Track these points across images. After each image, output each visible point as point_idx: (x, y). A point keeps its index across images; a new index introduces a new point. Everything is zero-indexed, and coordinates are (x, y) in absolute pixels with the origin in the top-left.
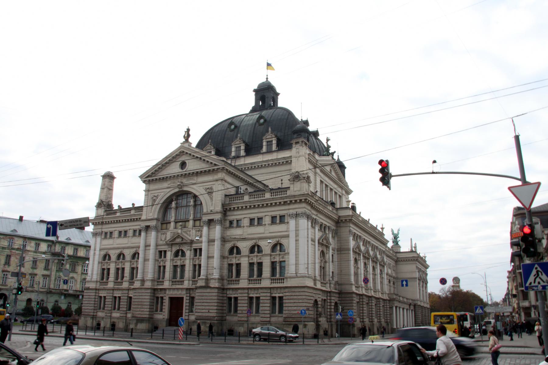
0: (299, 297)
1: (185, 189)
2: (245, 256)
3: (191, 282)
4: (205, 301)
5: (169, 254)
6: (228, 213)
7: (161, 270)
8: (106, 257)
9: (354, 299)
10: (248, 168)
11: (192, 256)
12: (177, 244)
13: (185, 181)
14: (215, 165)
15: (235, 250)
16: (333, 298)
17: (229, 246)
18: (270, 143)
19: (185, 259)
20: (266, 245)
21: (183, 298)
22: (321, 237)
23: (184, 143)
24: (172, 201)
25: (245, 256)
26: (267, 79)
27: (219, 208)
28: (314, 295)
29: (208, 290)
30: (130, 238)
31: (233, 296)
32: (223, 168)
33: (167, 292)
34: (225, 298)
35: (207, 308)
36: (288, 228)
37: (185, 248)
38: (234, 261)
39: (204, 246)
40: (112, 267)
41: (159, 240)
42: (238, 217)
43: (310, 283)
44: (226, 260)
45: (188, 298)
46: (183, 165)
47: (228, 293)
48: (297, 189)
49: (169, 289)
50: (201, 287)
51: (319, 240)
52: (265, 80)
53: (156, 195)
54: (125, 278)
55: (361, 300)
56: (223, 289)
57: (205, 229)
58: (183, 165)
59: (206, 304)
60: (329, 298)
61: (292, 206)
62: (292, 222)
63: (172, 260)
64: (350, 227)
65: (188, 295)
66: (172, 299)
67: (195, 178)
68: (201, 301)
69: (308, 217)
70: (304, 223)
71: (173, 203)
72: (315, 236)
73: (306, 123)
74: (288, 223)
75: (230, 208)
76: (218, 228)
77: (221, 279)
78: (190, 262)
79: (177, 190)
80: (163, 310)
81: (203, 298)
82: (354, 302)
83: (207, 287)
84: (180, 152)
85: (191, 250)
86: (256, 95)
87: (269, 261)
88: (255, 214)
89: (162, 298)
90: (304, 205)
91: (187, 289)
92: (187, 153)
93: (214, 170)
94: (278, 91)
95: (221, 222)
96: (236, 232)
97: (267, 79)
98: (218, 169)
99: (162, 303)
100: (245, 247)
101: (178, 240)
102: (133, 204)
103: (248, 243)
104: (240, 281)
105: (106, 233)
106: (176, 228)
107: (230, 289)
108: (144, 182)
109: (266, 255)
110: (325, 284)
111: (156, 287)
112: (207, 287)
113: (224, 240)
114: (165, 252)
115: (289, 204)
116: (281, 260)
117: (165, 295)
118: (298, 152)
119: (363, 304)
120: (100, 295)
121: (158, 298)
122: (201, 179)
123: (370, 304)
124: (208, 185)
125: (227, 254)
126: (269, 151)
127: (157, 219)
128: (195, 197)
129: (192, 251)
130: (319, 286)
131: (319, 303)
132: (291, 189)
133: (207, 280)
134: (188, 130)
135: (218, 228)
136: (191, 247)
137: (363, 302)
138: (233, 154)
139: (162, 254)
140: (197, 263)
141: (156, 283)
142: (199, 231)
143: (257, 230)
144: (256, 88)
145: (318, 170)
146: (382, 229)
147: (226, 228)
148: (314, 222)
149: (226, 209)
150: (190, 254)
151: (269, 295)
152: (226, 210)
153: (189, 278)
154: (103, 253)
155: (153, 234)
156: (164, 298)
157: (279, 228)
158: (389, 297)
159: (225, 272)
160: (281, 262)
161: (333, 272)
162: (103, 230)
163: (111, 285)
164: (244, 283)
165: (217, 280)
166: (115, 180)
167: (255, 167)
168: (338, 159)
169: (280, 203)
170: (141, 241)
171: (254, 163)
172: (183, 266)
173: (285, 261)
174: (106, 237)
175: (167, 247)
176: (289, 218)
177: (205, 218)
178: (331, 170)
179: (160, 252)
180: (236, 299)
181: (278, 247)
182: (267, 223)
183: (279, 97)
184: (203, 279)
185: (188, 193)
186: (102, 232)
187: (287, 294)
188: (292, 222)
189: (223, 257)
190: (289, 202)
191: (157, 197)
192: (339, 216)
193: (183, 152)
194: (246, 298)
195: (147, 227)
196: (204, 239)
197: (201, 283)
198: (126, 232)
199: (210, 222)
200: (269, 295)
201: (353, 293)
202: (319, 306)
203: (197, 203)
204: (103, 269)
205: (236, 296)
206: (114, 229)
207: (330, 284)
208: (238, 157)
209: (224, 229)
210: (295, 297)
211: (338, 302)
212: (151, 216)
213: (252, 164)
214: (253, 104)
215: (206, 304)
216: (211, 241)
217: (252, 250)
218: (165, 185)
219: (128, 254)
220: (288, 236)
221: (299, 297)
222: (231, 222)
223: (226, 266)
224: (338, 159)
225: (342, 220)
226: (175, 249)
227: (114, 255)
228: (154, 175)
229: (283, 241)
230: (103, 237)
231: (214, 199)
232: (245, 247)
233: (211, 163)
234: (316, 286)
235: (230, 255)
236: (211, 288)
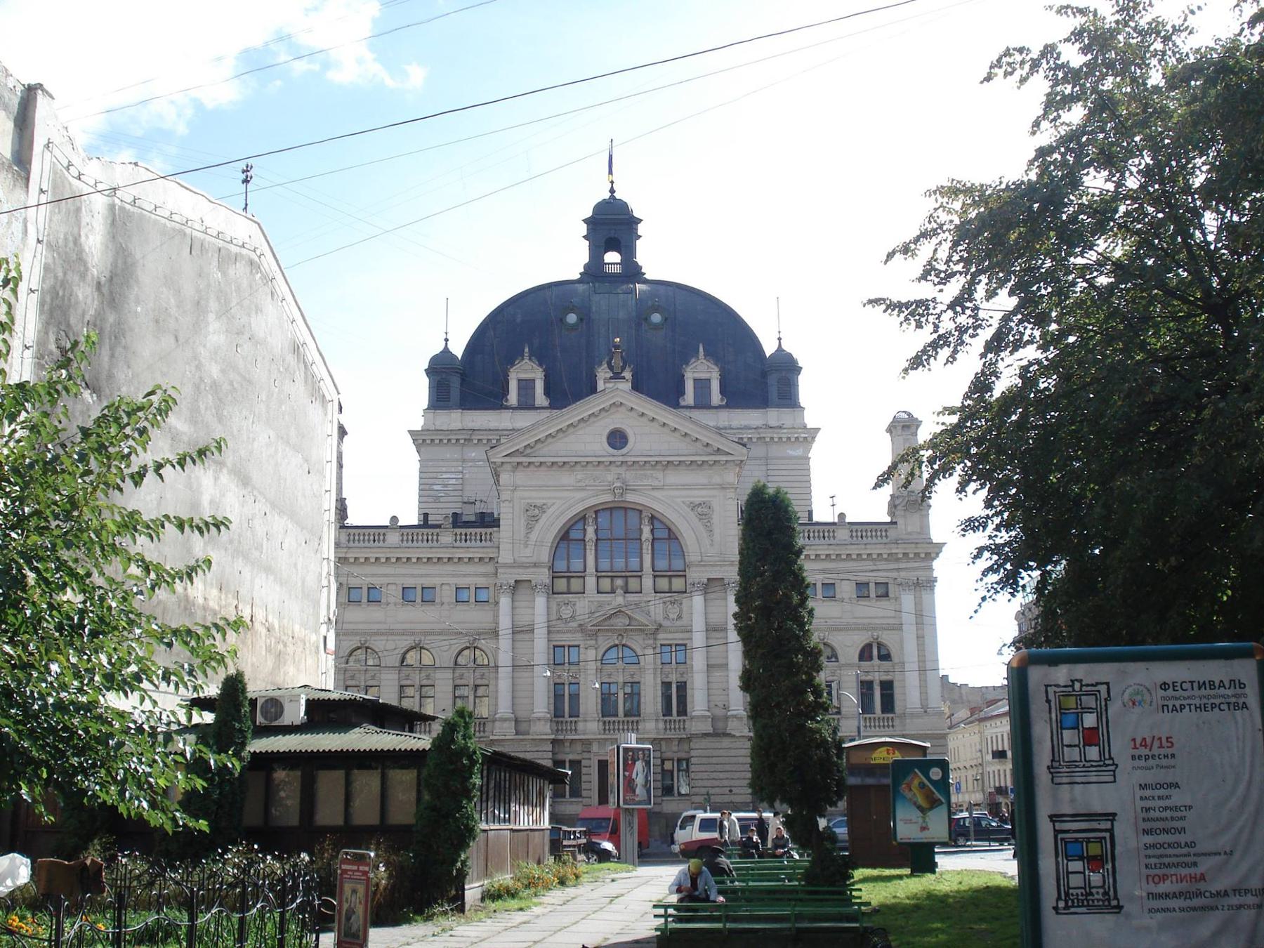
1: (631, 497)
3: (661, 725)
4: (719, 767)
13: (629, 476)
26: (612, 191)
29: (726, 742)
30: (391, 607)
33: (595, 748)
35: (726, 783)
37: (636, 643)
46: (617, 439)
52: (607, 195)
53: (539, 502)
58: (617, 439)
59: (721, 775)
62: (907, 600)
67: (660, 475)
68: (708, 768)
79: (606, 498)
80: (584, 793)
81: (714, 760)
87: (854, 679)
97: (612, 191)
101: (620, 622)
112: (719, 734)
115: (898, 560)
117: (586, 755)
122: (673, 477)
124: (698, 496)
140: (673, 678)
142: (673, 603)
144: (589, 214)
155: (540, 601)
156: (584, 763)
175: (579, 636)
183: (638, 242)
191: (542, 509)
203: (667, 536)
206: (386, 580)
212: (526, 554)
215: (721, 775)
217: (865, 654)
218: (567, 478)
220: (899, 627)
226: (604, 643)
229: (887, 638)
231: (717, 531)
236: (729, 735)
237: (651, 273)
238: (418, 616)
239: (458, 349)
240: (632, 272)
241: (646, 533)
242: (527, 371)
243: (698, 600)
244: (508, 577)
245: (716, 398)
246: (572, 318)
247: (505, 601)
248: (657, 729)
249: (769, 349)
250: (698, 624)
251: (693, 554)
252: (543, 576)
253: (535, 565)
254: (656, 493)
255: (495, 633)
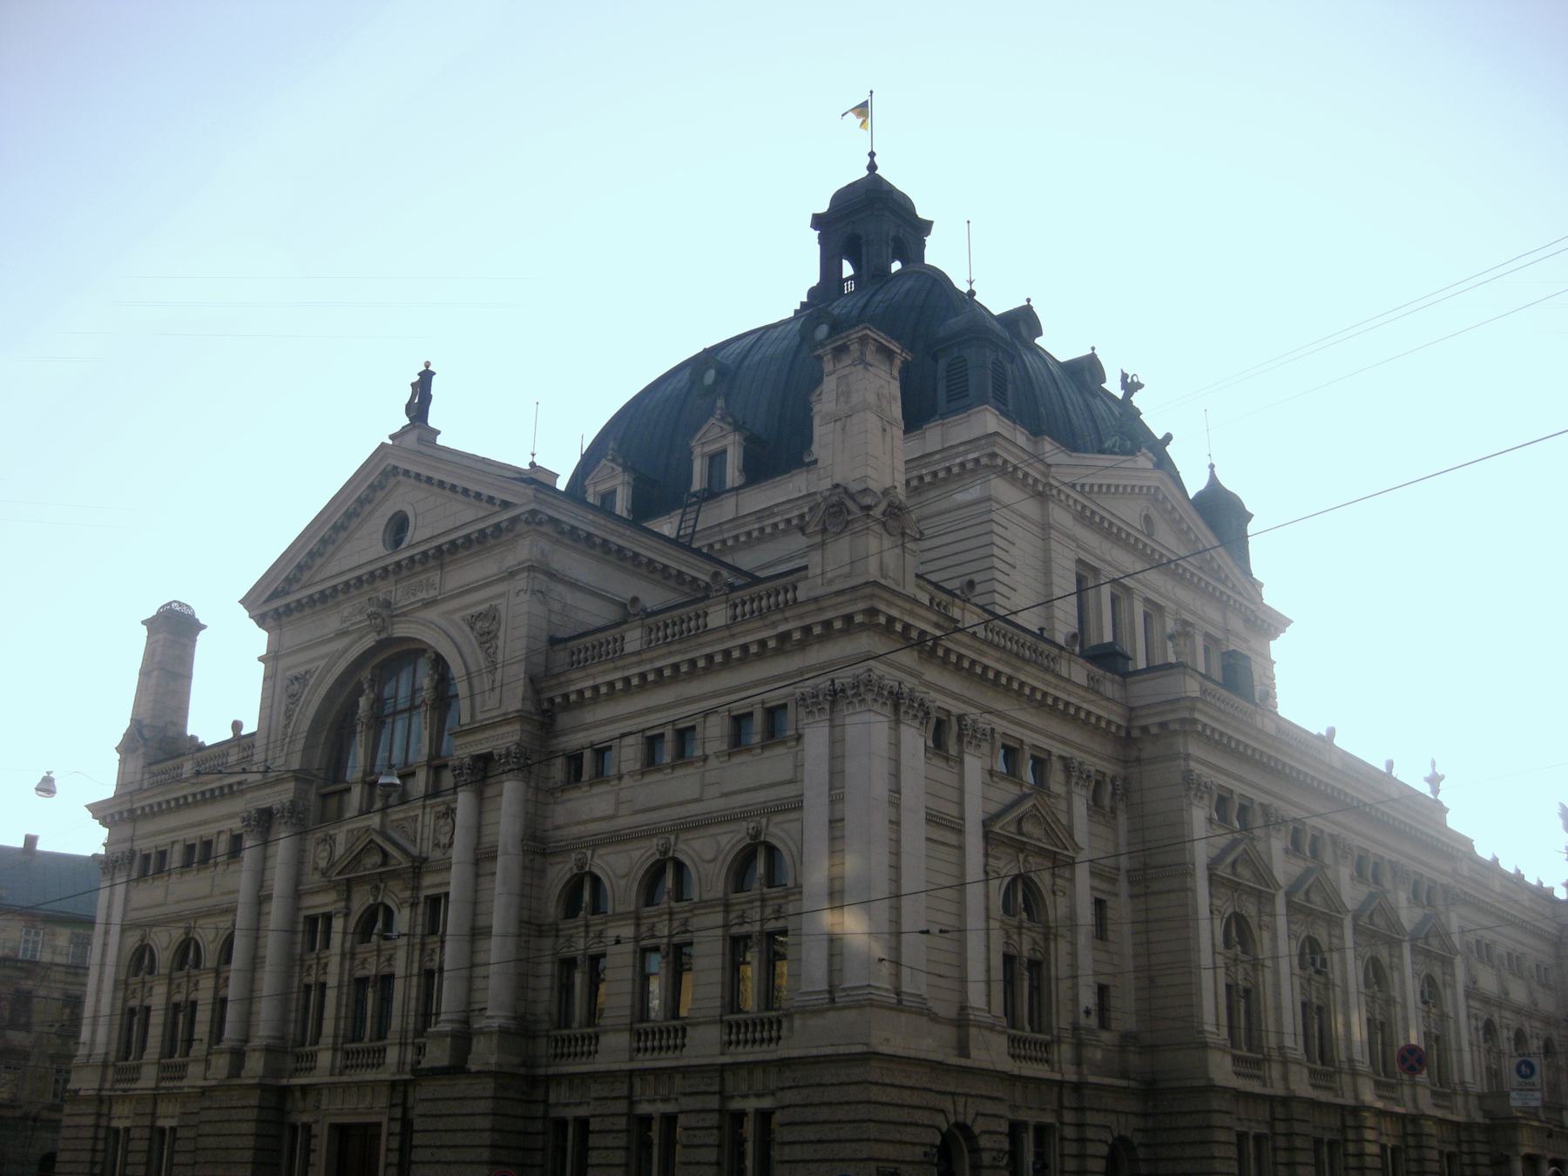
0: (841, 1114)
1: (400, 630)
2: (623, 916)
5: (338, 924)
6: (564, 720)
7: (305, 999)
8: (141, 960)
9: (1217, 1120)
10: (749, 534)
11: (419, 930)
12: (361, 880)
13: (398, 593)
14: (506, 505)
15: (582, 893)
16: (1097, 1118)
17: (560, 872)
19: (395, 948)
20: (708, 857)
21: (379, 1125)
22: (1225, 851)
23: (404, 431)
24: (359, 691)
25: (623, 916)
26: (872, 167)
27: (515, 698)
28: (948, 1104)
31: (570, 1113)
32: (534, 512)
34: (539, 1126)
36: (798, 766)
38: (581, 946)
39: (456, 882)
40: (158, 998)
41: (308, 868)
42: (599, 735)
43: (931, 1044)
44: (548, 943)
45: (397, 1127)
46: (398, 527)
47: (552, 1099)
48: (836, 563)
49: (332, 1086)
50: (435, 1072)
51: (987, 824)
54: (196, 1046)
55: (1281, 1127)
56: (533, 1081)
57: (464, 802)
58: (398, 527)
60: (1069, 1117)
61: (817, 655)
63: (348, 955)
64: (1188, 757)
65: (398, 1112)
66: (342, 1133)
67: (435, 576)
69: (897, 701)
70: (869, 728)
71: (362, 701)
72: (961, 804)
73: (1024, 321)
74: (799, 738)
75: (566, 696)
76: (510, 794)
77: (521, 1029)
78: (409, 963)
79: (369, 641)
82: (1222, 1136)
83: (457, 1069)
84: (385, 474)
85: (414, 905)
86: (823, 240)
88: (660, 708)
89: (307, 1127)
90: (865, 643)
91: (393, 1084)
92: (406, 473)
93: (497, 526)
94: (922, 213)
95: (526, 762)
96: (589, 808)
97: (872, 167)
98: (514, 520)
99: (308, 1151)
100: (620, 869)
102: (237, 726)
103: (636, 854)
104: (602, 1039)
105: (147, 857)
106: (365, 811)
107: (559, 1078)
108: (261, 621)
109: (705, 904)
110: (1257, 1064)
111: (284, 1082)
113: (538, 846)
114: (328, 918)
115: (803, 645)
116: (771, 925)
118: (848, 394)
119: (1290, 1149)
120: (115, 1123)
121: (294, 1128)
123: (1351, 1148)
124: (477, 602)
125: (552, 909)
127: (301, 777)
128: (439, 663)
129: (420, 909)
130: (991, 1052)
131: (984, 1142)
132: (815, 570)
133: (463, 1038)
134: (426, 377)
135: (510, 794)
136: (416, 888)
137: (1290, 1135)
138: (697, 484)
139: (315, 928)
141: (290, 1063)
143: (675, 789)
144: (823, 207)
145: (1060, 516)
146: (1435, 780)
147: (551, 792)
148: (944, 736)
149: (551, 700)
150: (412, 925)
151: (714, 1102)
152: (546, 711)
153: (404, 1031)
154: (133, 940)
156: (315, 1129)
157: (761, 770)
158: (1487, 1113)
159: (545, 997)
160: (771, 936)
161: (1102, 991)
162: (138, 845)
163: (148, 1078)
164: (614, 1052)
165: (495, 1038)
166: (202, 637)
167: (775, 525)
168: (1213, 480)
169: (762, 643)
170: (241, 880)
171: (768, 512)
172: (387, 980)
173: (784, 932)
174: (143, 874)
175: (332, 896)
176: (802, 712)
177: (462, 750)
178: (1148, 519)
179: (312, 921)
180: (583, 1123)
181: (759, 862)
182: (712, 748)
184: (442, 1035)
186: (132, 853)
187: (790, 1097)
188: (816, 737)
189: (530, 928)
190: (797, 636)
192: (1131, 709)
193: (396, 468)
194: (622, 1123)
195: (265, 820)
196: (460, 852)
197: (438, 1054)
198: (208, 844)
199: (482, 770)
200: (714, 1102)
201: (1211, 1088)
202: (986, 1158)
204: (132, 1011)
205: (582, 1112)
207: (1079, 1045)
208: (713, 492)
209: (540, 799)
210: (824, 1113)
211: (1137, 1139)
213: (760, 515)
214: (814, 278)
216: (483, 857)
219: (208, 937)
221: (841, 1114)
222: (575, 759)
223: (547, 968)
224: (1213, 480)
225: (1145, 729)
226: (362, 900)
227: (164, 942)
228: (295, 587)
229: (778, 832)
230: (134, 875)
232: (620, 869)
233: (491, 499)
234: (967, 1056)
235: (567, 917)
238: (189, 889)
248: (401, 1064)
253: (279, 781)
254: (432, 614)
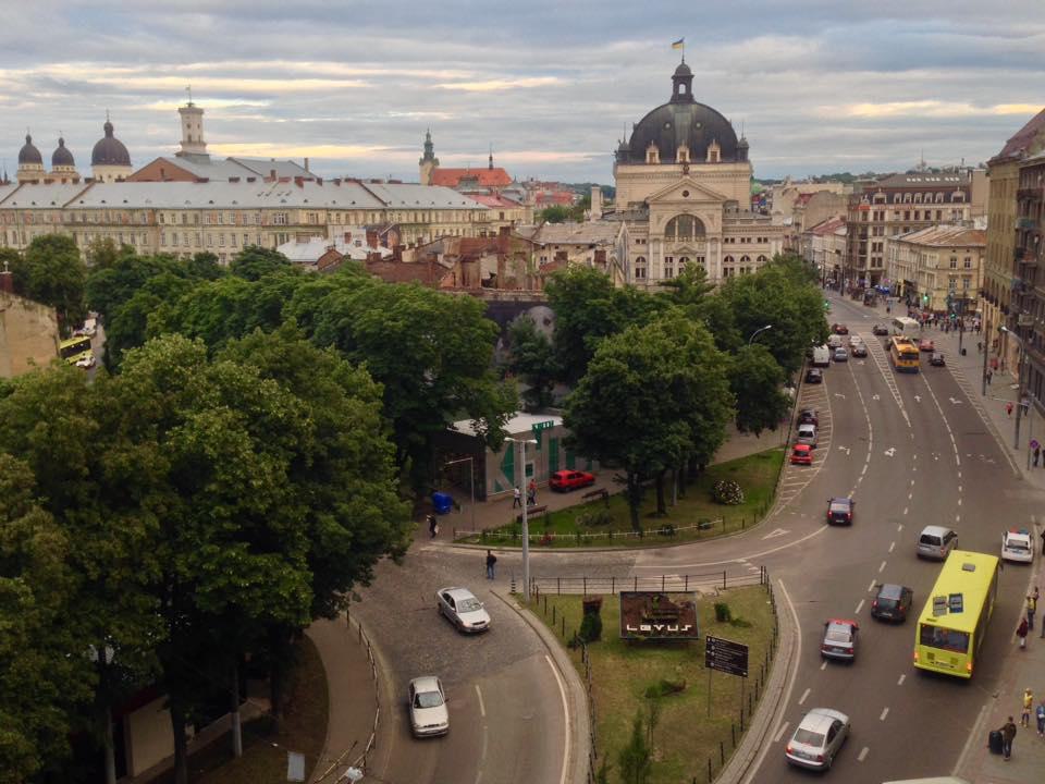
18: (714, 154)
46: (686, 194)
58: (686, 194)
62: (773, 243)
101: (685, 251)
124: (710, 212)
126: (714, 162)
128: (696, 218)
143: (746, 247)
144: (673, 73)
152: (724, 230)
157: (763, 246)
185: (692, 216)
212: (657, 231)
218: (670, 207)
226: (680, 257)
237: (697, 98)
239: (628, 141)
240: (688, 98)
241: (694, 224)
242: (653, 150)
243: (709, 244)
244: (651, 238)
245: (718, 159)
246: (668, 126)
247: (651, 245)
249: (739, 138)
250: (709, 250)
251: (707, 231)
252: (662, 237)
255: (648, 253)
